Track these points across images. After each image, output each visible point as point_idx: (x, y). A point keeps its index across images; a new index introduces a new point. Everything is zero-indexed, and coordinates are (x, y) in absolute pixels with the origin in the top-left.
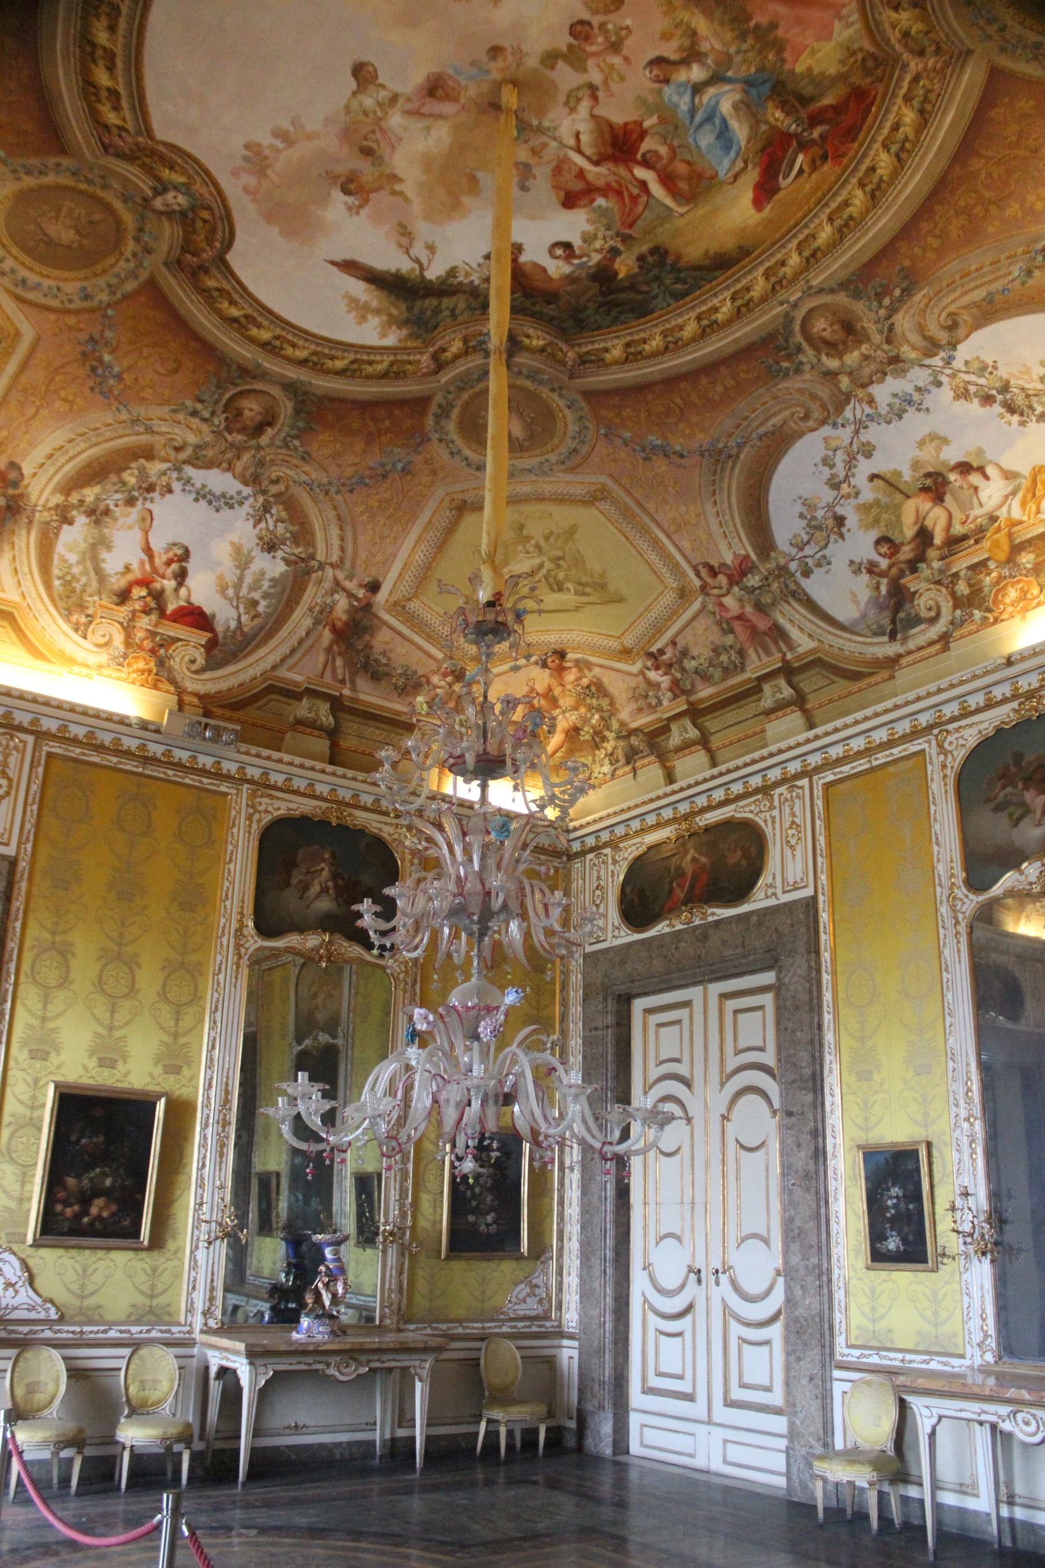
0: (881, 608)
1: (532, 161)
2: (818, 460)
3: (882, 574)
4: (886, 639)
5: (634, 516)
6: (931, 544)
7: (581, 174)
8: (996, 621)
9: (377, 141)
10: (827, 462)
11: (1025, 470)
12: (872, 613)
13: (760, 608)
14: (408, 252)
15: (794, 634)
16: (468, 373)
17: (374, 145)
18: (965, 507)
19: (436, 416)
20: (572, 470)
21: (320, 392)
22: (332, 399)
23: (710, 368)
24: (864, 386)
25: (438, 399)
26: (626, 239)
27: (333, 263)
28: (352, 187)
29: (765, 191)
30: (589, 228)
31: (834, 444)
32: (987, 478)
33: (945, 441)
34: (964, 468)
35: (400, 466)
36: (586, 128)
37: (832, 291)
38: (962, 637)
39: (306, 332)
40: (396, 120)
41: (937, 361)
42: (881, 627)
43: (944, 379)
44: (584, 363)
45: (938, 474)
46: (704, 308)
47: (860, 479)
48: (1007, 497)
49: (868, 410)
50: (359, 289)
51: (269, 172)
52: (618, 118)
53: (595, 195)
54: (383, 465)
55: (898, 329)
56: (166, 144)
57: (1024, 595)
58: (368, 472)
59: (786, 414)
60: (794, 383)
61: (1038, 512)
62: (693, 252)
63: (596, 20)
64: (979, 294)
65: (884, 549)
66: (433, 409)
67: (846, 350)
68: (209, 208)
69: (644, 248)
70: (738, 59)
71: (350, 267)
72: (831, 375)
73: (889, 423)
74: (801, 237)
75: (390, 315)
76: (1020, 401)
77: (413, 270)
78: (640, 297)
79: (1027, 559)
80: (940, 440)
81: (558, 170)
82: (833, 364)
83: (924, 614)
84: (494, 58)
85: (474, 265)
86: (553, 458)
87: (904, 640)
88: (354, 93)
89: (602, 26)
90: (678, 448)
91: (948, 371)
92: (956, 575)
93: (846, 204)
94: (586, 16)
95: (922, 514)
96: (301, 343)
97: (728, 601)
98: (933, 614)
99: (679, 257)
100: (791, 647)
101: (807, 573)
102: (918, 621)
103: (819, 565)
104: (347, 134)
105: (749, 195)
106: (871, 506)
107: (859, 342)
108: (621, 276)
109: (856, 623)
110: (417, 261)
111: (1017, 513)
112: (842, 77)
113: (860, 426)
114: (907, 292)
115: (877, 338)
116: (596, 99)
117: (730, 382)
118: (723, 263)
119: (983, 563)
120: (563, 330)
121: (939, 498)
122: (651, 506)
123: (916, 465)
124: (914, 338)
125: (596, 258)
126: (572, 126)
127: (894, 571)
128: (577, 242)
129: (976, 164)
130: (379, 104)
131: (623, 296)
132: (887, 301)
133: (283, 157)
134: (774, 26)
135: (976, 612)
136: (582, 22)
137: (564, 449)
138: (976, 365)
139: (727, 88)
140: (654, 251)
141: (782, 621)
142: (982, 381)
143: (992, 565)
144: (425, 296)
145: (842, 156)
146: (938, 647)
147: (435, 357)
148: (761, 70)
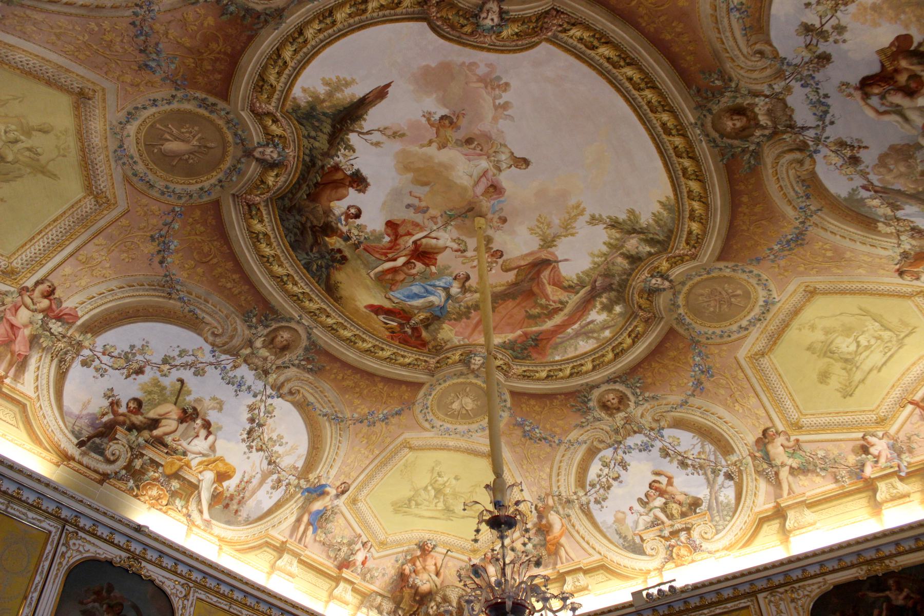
0: (92, 425)
1: (427, 215)
2: (183, 347)
3: (115, 413)
4: (76, 441)
5: (86, 227)
6: (151, 430)
7: (409, 234)
8: (136, 496)
9: (474, 149)
10: (182, 353)
11: (218, 454)
12: (86, 421)
13: (33, 340)
14: (378, 130)
15: (29, 375)
16: (245, 128)
17: (473, 146)
18: (184, 435)
19: (203, 100)
20: (127, 179)
21: (263, 32)
22: (251, 38)
23: (246, 279)
24: (245, 361)
25: (221, 104)
26: (356, 246)
27: (388, 85)
28: (447, 122)
29: (377, 310)
30: (368, 230)
31: (199, 354)
32: (206, 438)
33: (220, 409)
34: (207, 425)
35: (153, 64)
36: (441, 243)
37: (309, 338)
38: (114, 486)
39: (329, 43)
40: (484, 164)
41: (269, 391)
42: (81, 434)
43: (259, 397)
44: (249, 206)
45: (198, 414)
46: (297, 278)
47: (175, 374)
48: (200, 453)
49: (228, 367)
50: (359, 91)
51: (482, 85)
52: (439, 257)
53: (393, 238)
54: (158, 53)
55: (286, 370)
56: (536, 44)
57: (158, 498)
58: (152, 40)
59: (216, 324)
60: (240, 326)
61: (200, 472)
62: (340, 276)
63: (500, 261)
64: (311, 399)
65: (132, 405)
66: (212, 99)
67: (270, 350)
68: (472, 34)
69: (347, 253)
70: (457, 305)
71: (381, 93)
72: (250, 343)
73: (223, 378)
74: (346, 324)
75: (324, 101)
76: (255, 435)
77: (362, 128)
78: (308, 246)
79: (175, 485)
80: (220, 406)
81: (417, 225)
82: (258, 343)
83: (108, 453)
84: (500, 218)
85: (352, 162)
86: (140, 168)
87: (84, 454)
88: (513, 154)
89: (497, 262)
90: (169, 260)
91: (264, 398)
92: (142, 455)
93: (364, 341)
94: (504, 258)
95: (167, 416)
96: (321, 36)
97: (24, 315)
98: (112, 458)
99: (338, 269)
100: (16, 378)
101: (85, 364)
102: (101, 453)
103: (97, 370)
104: (488, 137)
105: (376, 303)
106: (159, 386)
107: (276, 354)
108: (327, 239)
109: (70, 414)
110: (368, 133)
111: (194, 463)
112: (435, 339)
113: (216, 365)
114: (310, 371)
115: (279, 362)
116: (456, 251)
117: (236, 291)
118: (331, 290)
119: (158, 465)
120: (282, 198)
121: (182, 420)
122: (100, 240)
123: (198, 400)
124: (282, 379)
125: (345, 229)
126: (445, 238)
127: (121, 418)
128: (358, 221)
129: (380, 385)
130: (498, 161)
131: (310, 239)
132: (303, 363)
133: (489, 99)
134: (468, 318)
135: (132, 481)
136: (502, 256)
137: (151, 177)
138: (270, 409)
139: (443, 300)
140: (344, 259)
141: (33, 363)
142: (262, 414)
143: (160, 470)
144: (333, 126)
145: (392, 339)
146: (97, 477)
147: (268, 114)
148: (448, 312)
